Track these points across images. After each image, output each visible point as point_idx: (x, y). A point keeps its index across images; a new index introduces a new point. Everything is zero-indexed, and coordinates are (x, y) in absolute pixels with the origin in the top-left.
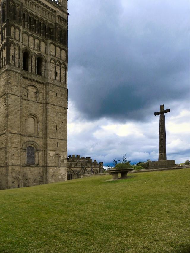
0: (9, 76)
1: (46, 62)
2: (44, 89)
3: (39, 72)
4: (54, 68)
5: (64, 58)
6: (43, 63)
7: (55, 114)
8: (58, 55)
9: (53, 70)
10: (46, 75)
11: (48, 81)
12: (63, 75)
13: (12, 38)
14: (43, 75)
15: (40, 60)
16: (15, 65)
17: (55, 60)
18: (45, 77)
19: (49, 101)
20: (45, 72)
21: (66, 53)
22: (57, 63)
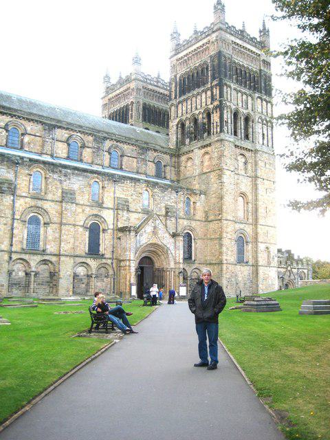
1: (253, 122)
3: (247, 137)
6: (251, 123)
7: (265, 190)
8: (264, 111)
9: (260, 131)
12: (270, 136)
13: (225, 100)
14: (251, 139)
15: (247, 119)
18: (253, 142)
19: (259, 175)
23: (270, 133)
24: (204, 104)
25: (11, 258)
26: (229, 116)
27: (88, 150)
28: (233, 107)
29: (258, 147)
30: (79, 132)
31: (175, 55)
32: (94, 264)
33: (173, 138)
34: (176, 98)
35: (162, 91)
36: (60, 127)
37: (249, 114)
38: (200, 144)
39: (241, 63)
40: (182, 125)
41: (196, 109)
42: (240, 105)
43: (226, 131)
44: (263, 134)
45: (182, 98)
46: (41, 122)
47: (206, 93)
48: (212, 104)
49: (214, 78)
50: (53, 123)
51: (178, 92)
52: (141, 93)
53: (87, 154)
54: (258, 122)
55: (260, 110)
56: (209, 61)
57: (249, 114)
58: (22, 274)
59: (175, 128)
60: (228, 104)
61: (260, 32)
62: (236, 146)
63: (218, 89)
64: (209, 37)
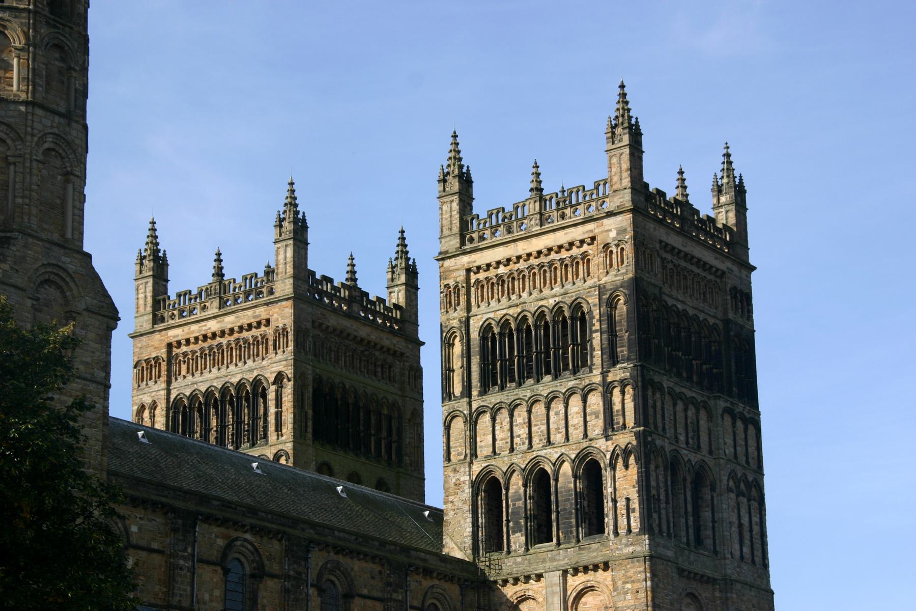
0: (656, 579)
1: (713, 489)
2: (718, 602)
4: (736, 511)
5: (753, 458)
6: (707, 494)
8: (740, 450)
9: (734, 519)
10: (717, 541)
11: (729, 571)
14: (709, 542)
16: (661, 532)
17: (736, 474)
18: (716, 552)
20: (713, 527)
21: (756, 434)
22: (742, 485)
23: (756, 519)
24: (576, 433)
27: (271, 584)
29: (730, 570)
30: (253, 529)
31: (465, 253)
34: (467, 391)
35: (364, 332)
36: (209, 519)
37: (703, 465)
38: (568, 555)
39: (680, 306)
42: (682, 438)
44: (740, 525)
45: (494, 398)
46: (164, 505)
47: (584, 400)
48: (607, 438)
49: (612, 358)
50: (191, 506)
52: (309, 343)
54: (730, 490)
55: (729, 451)
56: (594, 300)
57: (703, 465)
59: (467, 491)
60: (659, 442)
61: (719, 190)
62: (681, 571)
63: (629, 398)
64: (590, 226)
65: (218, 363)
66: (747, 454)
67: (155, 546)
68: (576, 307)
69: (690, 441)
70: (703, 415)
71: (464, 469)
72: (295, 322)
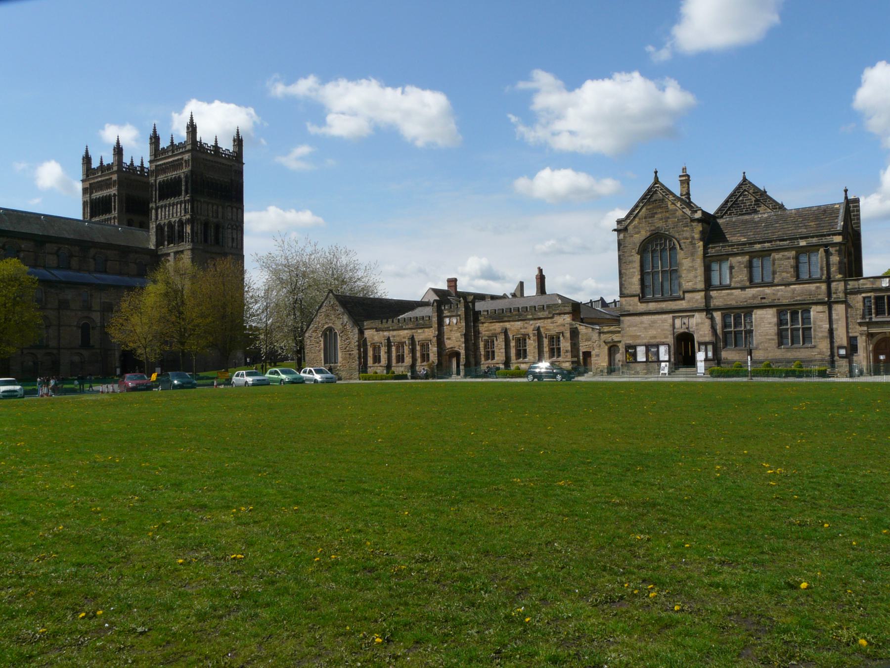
1: (223, 228)
3: (217, 241)
15: (217, 227)
22: (234, 227)
23: (239, 236)
24: (179, 214)
25: (22, 353)
26: (199, 227)
28: (204, 218)
32: (86, 353)
33: (153, 239)
39: (212, 177)
40: (160, 228)
41: (173, 216)
42: (211, 215)
43: (195, 241)
44: (233, 239)
45: (161, 203)
48: (184, 216)
49: (186, 193)
51: (157, 198)
53: (74, 262)
58: (31, 363)
60: (198, 217)
65: (102, 190)
66: (237, 218)
67: (31, 250)
68: (179, 177)
69: (214, 215)
70: (220, 207)
71: (154, 223)
72: (118, 178)
